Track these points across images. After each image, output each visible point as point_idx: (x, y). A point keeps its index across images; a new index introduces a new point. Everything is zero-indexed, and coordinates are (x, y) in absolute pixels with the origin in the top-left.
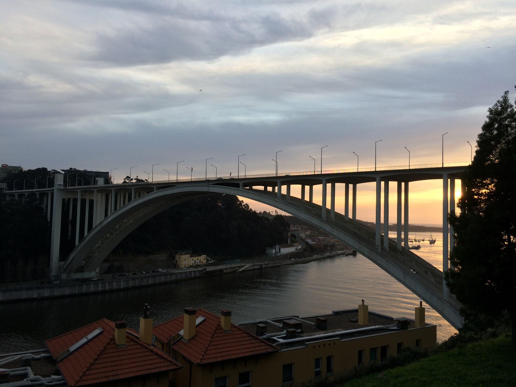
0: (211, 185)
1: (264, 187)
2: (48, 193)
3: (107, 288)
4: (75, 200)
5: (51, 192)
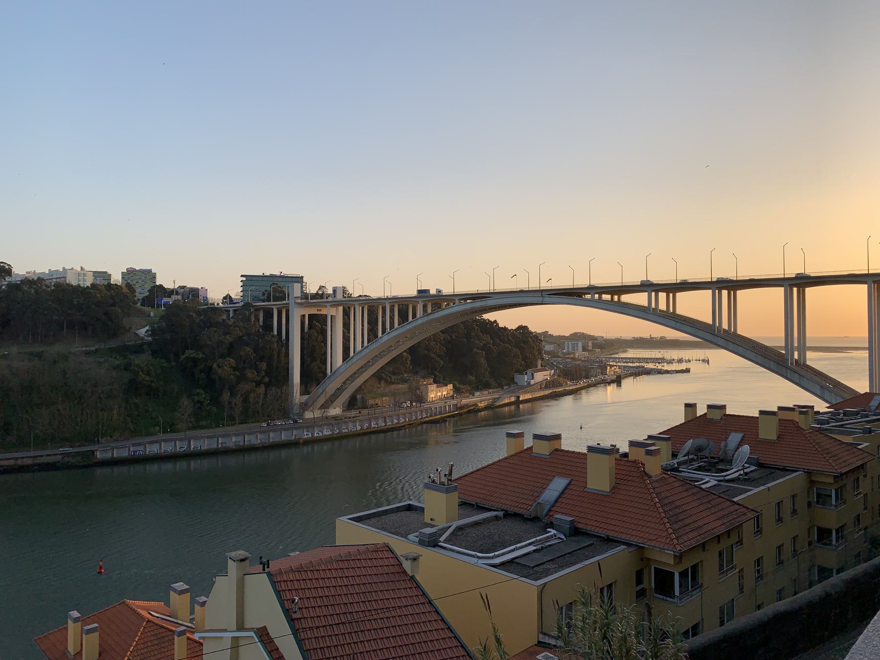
0: (548, 296)
1: (610, 296)
2: (273, 309)
5: (277, 307)
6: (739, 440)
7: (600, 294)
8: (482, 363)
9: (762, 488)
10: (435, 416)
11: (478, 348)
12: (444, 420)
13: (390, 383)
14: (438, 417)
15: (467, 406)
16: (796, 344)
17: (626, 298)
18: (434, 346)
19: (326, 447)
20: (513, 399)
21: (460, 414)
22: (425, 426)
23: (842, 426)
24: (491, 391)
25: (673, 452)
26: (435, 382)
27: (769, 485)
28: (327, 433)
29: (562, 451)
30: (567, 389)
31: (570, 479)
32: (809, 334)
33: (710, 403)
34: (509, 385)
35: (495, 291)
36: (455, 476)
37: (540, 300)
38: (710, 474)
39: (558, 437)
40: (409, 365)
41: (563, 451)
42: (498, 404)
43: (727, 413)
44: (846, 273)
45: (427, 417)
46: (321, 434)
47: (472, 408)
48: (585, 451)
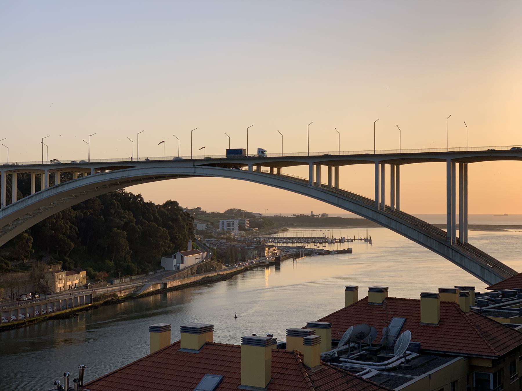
0: (200, 167)
1: (269, 168)
6: (400, 325)
7: (259, 166)
8: (123, 245)
9: (423, 376)
10: (63, 310)
11: (118, 228)
12: (74, 314)
13: (5, 271)
14: (68, 310)
15: (103, 296)
16: (458, 222)
17: (287, 171)
18: (63, 225)
20: (159, 287)
21: (96, 307)
22: (50, 322)
23: (500, 308)
24: (133, 277)
25: (333, 340)
26: (64, 268)
27: (430, 373)
29: (214, 345)
30: (221, 273)
31: (222, 376)
32: (471, 211)
33: (372, 286)
34: (155, 270)
35: (140, 160)
36: (85, 382)
37: (191, 171)
38: (370, 363)
39: (209, 329)
40: (30, 249)
41: (215, 344)
42: (141, 293)
43: (389, 296)
44: (219, 157)
45: (53, 311)
47: (110, 299)
48: (239, 343)
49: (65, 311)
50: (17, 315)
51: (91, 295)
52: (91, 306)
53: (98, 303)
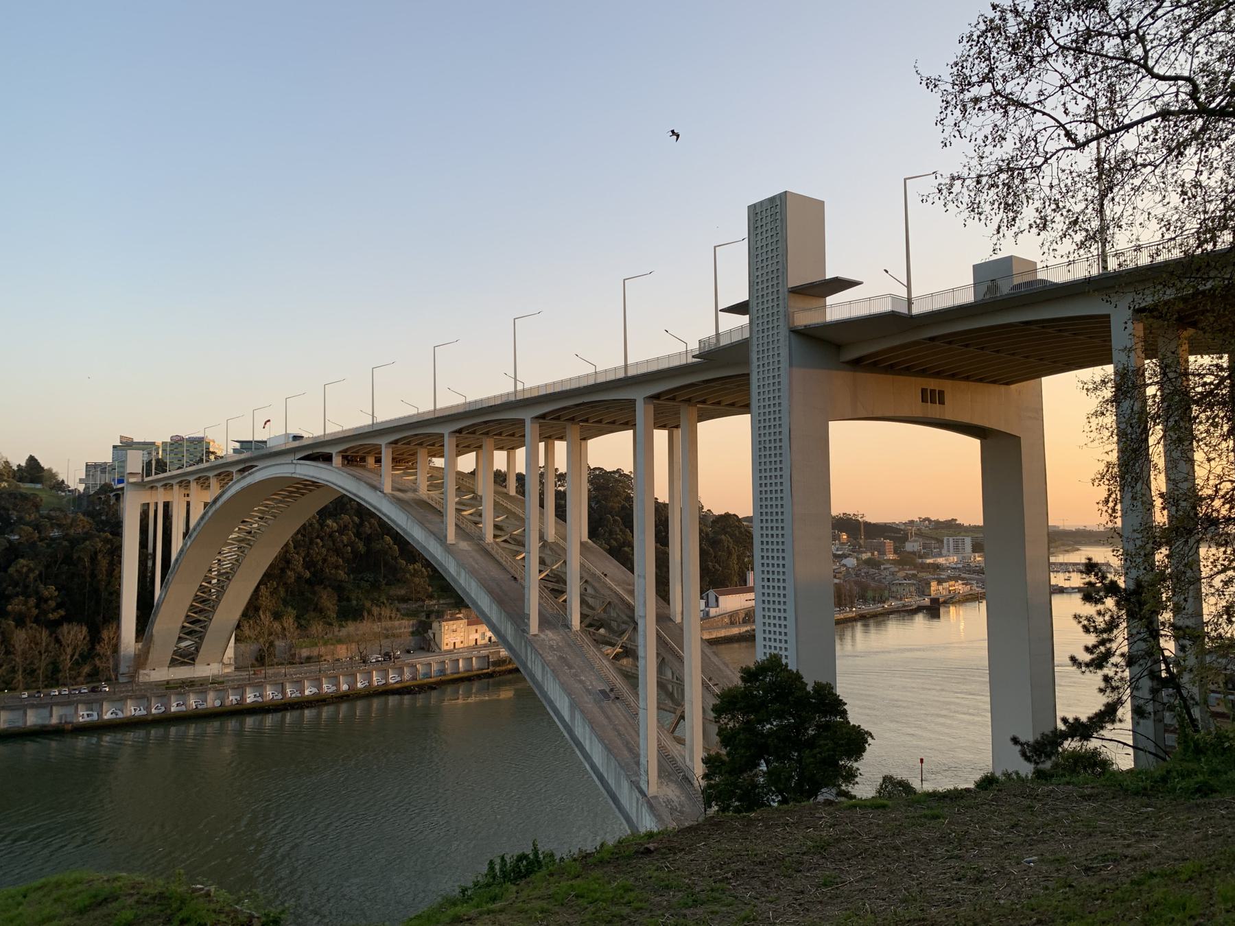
3: (345, 687)
4: (156, 504)
19: (130, 737)
21: (490, 675)
28: (138, 713)
46: (121, 715)
49: (426, 681)
50: (320, 687)
51: (488, 656)
52: (487, 673)
53: (503, 668)
